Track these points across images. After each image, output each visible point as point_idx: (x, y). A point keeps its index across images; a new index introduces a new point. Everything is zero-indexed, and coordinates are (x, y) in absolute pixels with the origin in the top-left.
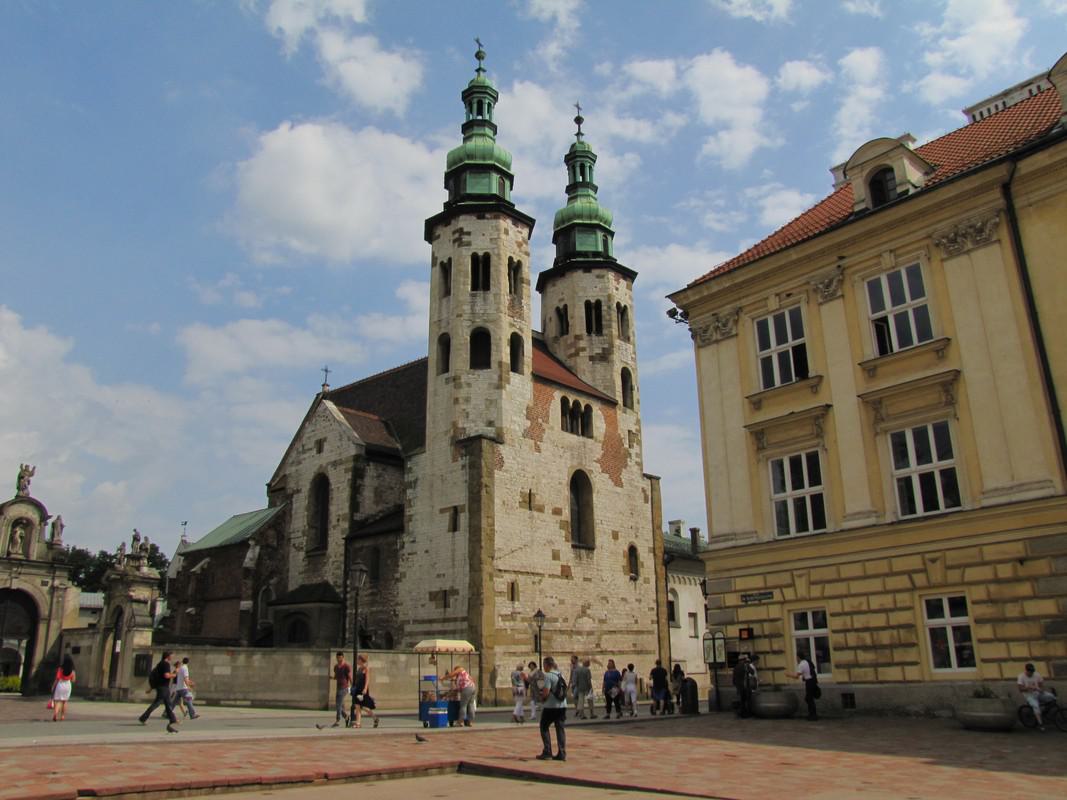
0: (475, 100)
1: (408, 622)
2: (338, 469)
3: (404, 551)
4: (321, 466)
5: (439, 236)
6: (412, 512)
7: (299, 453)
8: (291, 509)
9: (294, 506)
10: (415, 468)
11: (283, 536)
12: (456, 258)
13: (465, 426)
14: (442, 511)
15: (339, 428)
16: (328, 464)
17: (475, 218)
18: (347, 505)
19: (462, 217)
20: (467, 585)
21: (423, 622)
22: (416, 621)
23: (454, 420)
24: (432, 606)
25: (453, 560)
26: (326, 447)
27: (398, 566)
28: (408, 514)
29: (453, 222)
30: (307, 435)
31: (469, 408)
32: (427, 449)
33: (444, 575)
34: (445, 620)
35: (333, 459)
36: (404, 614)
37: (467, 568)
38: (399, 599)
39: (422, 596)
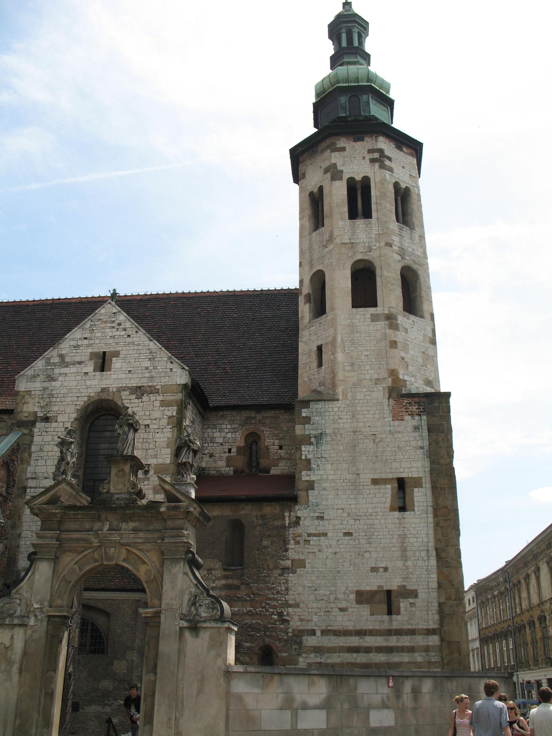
0: (357, 30)
1: (313, 633)
2: (145, 398)
3: (299, 530)
4: (103, 390)
5: (343, 149)
6: (313, 478)
7: (48, 363)
8: (32, 441)
9: (36, 439)
10: (316, 419)
11: (15, 480)
12: (378, 179)
13: (406, 378)
14: (375, 482)
15: (147, 342)
16: (120, 390)
17: (394, 146)
18: (169, 451)
19: (381, 139)
20: (435, 585)
21: (347, 633)
22: (325, 632)
23: (393, 368)
24: (365, 610)
25: (404, 550)
26: (116, 363)
27: (287, 550)
28: (304, 478)
29: (366, 139)
30: (73, 343)
31: (408, 357)
32: (340, 397)
33: (386, 569)
34: (389, 633)
35: (134, 383)
36: (301, 620)
37: (433, 562)
38: (290, 598)
39: (341, 596)
